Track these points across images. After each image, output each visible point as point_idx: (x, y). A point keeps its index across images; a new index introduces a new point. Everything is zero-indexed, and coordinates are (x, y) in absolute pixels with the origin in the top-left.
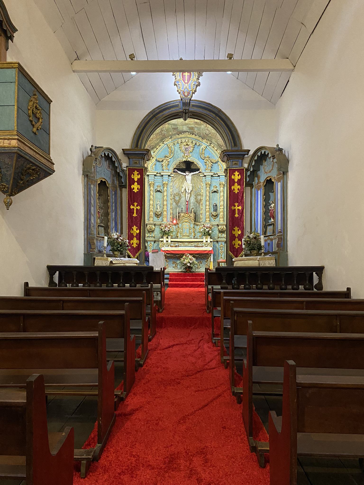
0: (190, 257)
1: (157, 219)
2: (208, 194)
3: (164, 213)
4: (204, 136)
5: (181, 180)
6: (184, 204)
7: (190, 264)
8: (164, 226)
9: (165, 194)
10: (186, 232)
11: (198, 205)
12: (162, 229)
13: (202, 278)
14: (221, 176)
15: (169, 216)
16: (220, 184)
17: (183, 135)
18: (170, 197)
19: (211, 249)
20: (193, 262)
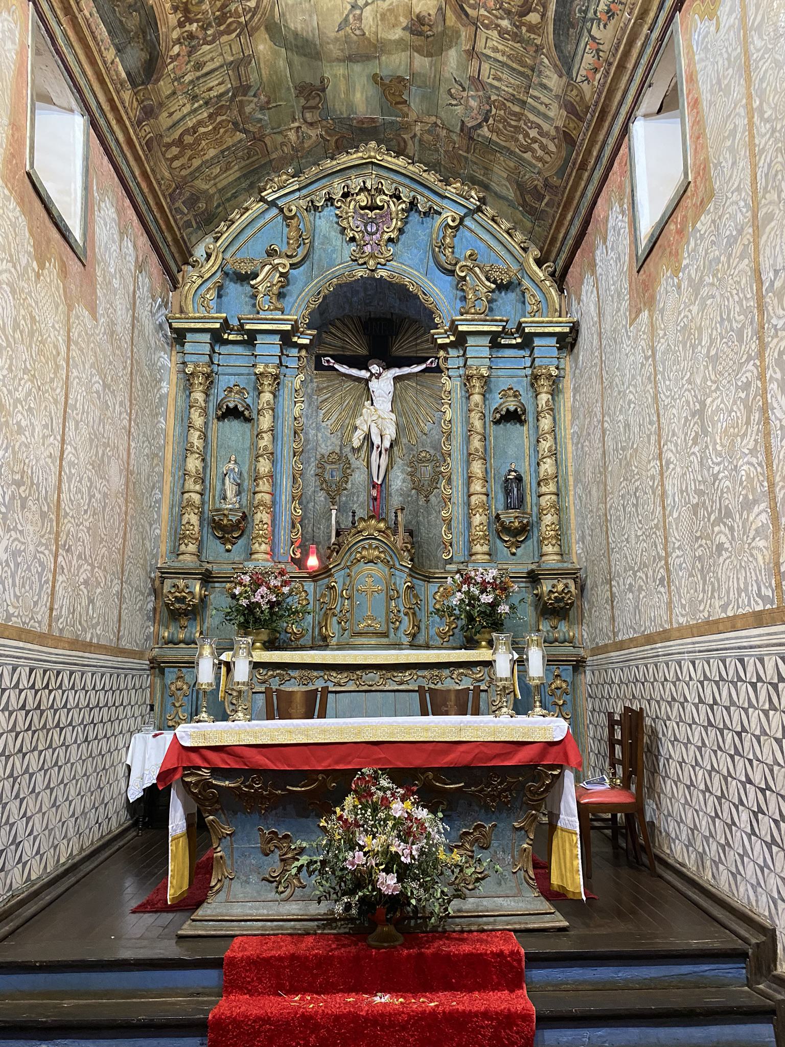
0: (398, 809)
1: (221, 548)
2: (478, 424)
3: (259, 516)
4: (454, 156)
6: (363, 497)
7: (404, 872)
8: (246, 579)
9: (265, 422)
10: (371, 613)
12: (234, 596)
14: (537, 342)
15: (283, 535)
16: (536, 377)
17: (354, 158)
19: (555, 728)
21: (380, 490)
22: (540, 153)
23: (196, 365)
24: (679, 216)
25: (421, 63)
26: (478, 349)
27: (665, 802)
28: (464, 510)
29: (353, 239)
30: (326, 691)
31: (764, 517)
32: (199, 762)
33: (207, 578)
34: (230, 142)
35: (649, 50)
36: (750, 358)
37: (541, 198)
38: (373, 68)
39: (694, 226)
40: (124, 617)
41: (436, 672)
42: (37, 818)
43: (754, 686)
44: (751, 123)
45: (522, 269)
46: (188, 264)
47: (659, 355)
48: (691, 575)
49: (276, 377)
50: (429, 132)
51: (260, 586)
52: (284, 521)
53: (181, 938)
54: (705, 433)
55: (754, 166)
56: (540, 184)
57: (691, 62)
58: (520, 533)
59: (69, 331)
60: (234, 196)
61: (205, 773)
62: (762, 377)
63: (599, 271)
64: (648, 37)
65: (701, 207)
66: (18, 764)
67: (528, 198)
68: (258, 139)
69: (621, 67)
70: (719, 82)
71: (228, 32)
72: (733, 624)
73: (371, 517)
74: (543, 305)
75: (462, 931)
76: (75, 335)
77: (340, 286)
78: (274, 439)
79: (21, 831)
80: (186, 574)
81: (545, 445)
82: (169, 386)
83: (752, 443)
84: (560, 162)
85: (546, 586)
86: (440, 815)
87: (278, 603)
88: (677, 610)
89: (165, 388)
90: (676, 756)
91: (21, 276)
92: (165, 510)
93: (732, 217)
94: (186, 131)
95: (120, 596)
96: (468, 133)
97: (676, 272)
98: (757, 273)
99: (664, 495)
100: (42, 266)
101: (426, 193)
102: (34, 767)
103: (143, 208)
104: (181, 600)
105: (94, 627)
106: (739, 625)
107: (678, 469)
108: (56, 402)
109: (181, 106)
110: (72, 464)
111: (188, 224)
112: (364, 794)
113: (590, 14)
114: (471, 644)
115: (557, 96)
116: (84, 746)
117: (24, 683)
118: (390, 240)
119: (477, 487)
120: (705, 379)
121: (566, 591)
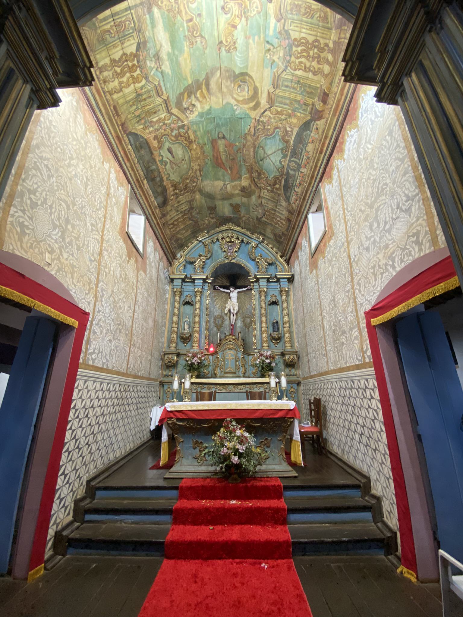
0: (238, 433)
1: (183, 345)
2: (264, 305)
5: (224, 299)
6: (228, 329)
7: (240, 456)
8: (191, 355)
9: (198, 306)
10: (231, 365)
11: (247, 330)
12: (186, 361)
13: (277, 510)
14: (281, 280)
15: (202, 341)
16: (281, 291)
17: (225, 227)
18: (204, 313)
19: (291, 404)
20: (248, 449)
21: (233, 327)
22: (280, 224)
23: (177, 289)
24: (324, 241)
25: (244, 200)
26: (263, 283)
27: (330, 431)
28: (259, 333)
29: (225, 251)
30: (215, 392)
31: (357, 333)
32: (173, 416)
33: (178, 355)
34: (188, 223)
35: (312, 194)
36: (348, 283)
37: (281, 238)
38: (230, 201)
39: (329, 243)
40: (152, 368)
41: (252, 386)
42: (119, 436)
43: (357, 390)
44: (344, 213)
45: (276, 259)
46: (175, 259)
47: (319, 283)
48: (334, 353)
49: (201, 292)
50: (247, 219)
51: (195, 357)
52: (203, 336)
53: (165, 478)
54: (336, 306)
55: (346, 225)
56: (281, 233)
57: (325, 196)
58: (278, 340)
59: (137, 279)
60: (189, 239)
61: (175, 420)
62: (353, 288)
63: (300, 258)
64: (312, 190)
65: (330, 238)
66: (114, 417)
67: (277, 238)
68: (196, 222)
69: (304, 199)
70: (334, 201)
71: (187, 192)
72: (349, 369)
73: (230, 335)
74: (283, 269)
75: (261, 477)
76: (139, 279)
77: (221, 265)
78: (200, 311)
79: (114, 440)
80: (172, 353)
81: (285, 312)
82: (168, 296)
83: (351, 310)
84: (286, 227)
85: (287, 357)
86: (253, 435)
87: (201, 363)
88: (330, 364)
89: (167, 296)
90: (333, 415)
91: (123, 262)
92: (166, 333)
93: (340, 240)
94: (175, 220)
95: (150, 360)
96: (259, 219)
97: (324, 257)
98: (349, 256)
99: (323, 327)
100: (130, 259)
101: (247, 237)
102: (119, 418)
103: (162, 242)
104: (170, 362)
105: (142, 371)
106: (351, 369)
107: (328, 319)
108: (132, 299)
109: (173, 214)
110: (136, 319)
111: (175, 247)
112: (227, 427)
113: (294, 184)
114: (263, 376)
115: (285, 208)
116: (136, 411)
117: (117, 389)
118: (236, 251)
119: (264, 325)
120: (334, 290)
121: (293, 359)
